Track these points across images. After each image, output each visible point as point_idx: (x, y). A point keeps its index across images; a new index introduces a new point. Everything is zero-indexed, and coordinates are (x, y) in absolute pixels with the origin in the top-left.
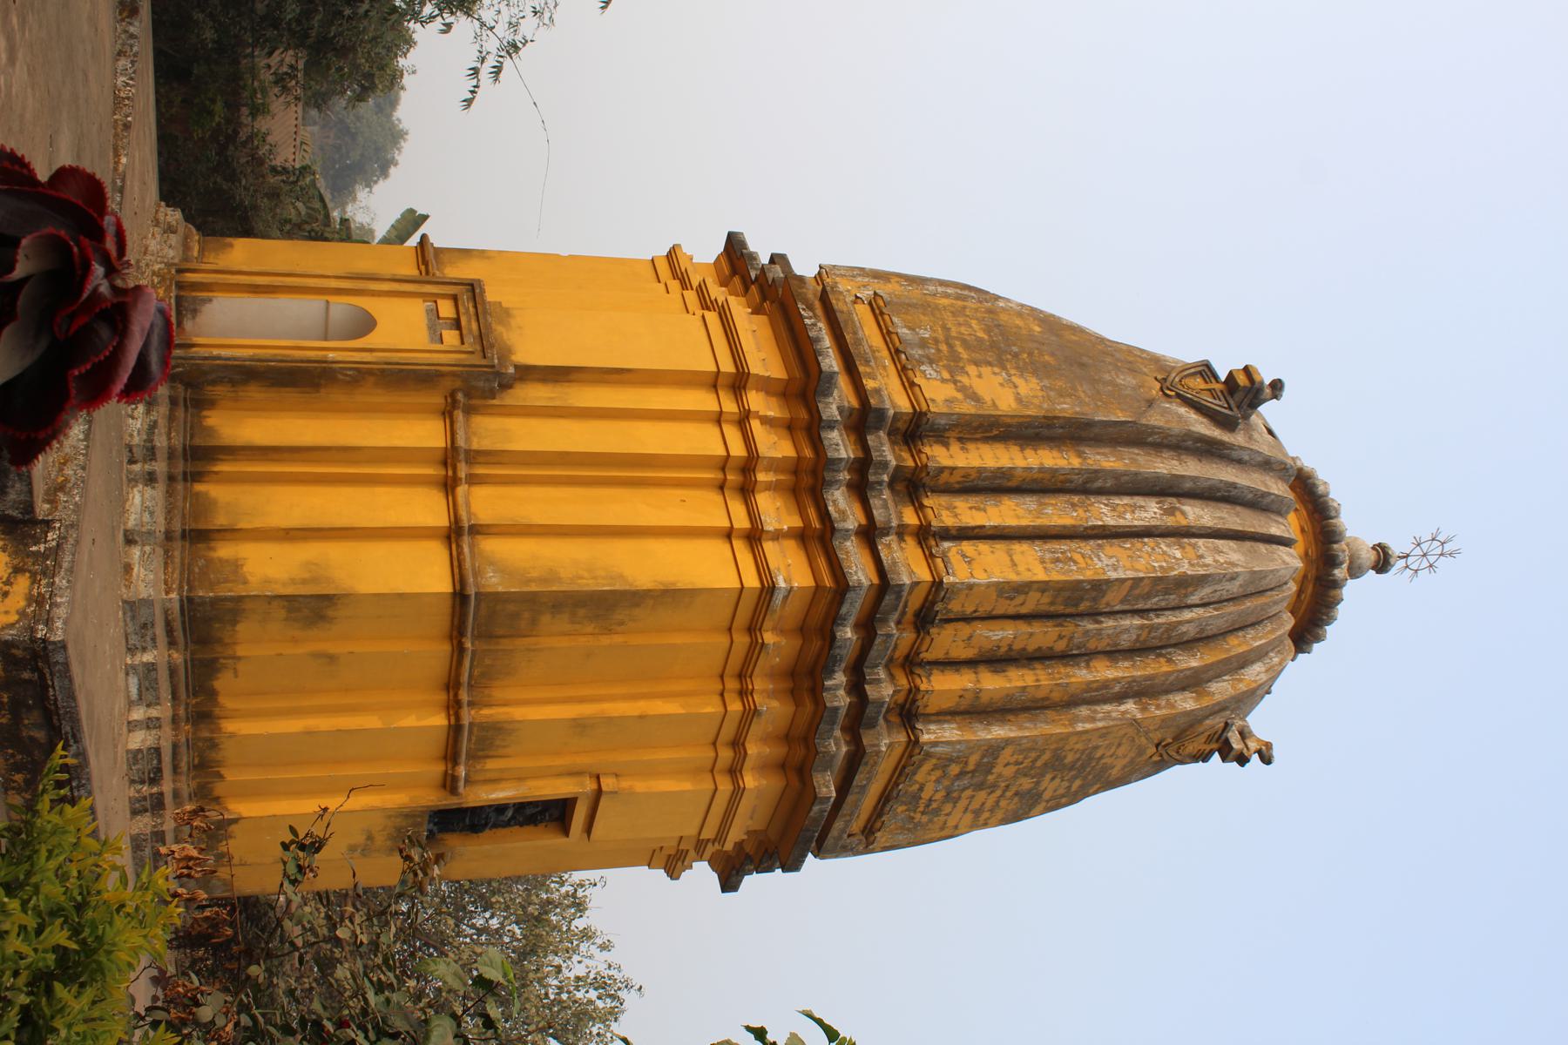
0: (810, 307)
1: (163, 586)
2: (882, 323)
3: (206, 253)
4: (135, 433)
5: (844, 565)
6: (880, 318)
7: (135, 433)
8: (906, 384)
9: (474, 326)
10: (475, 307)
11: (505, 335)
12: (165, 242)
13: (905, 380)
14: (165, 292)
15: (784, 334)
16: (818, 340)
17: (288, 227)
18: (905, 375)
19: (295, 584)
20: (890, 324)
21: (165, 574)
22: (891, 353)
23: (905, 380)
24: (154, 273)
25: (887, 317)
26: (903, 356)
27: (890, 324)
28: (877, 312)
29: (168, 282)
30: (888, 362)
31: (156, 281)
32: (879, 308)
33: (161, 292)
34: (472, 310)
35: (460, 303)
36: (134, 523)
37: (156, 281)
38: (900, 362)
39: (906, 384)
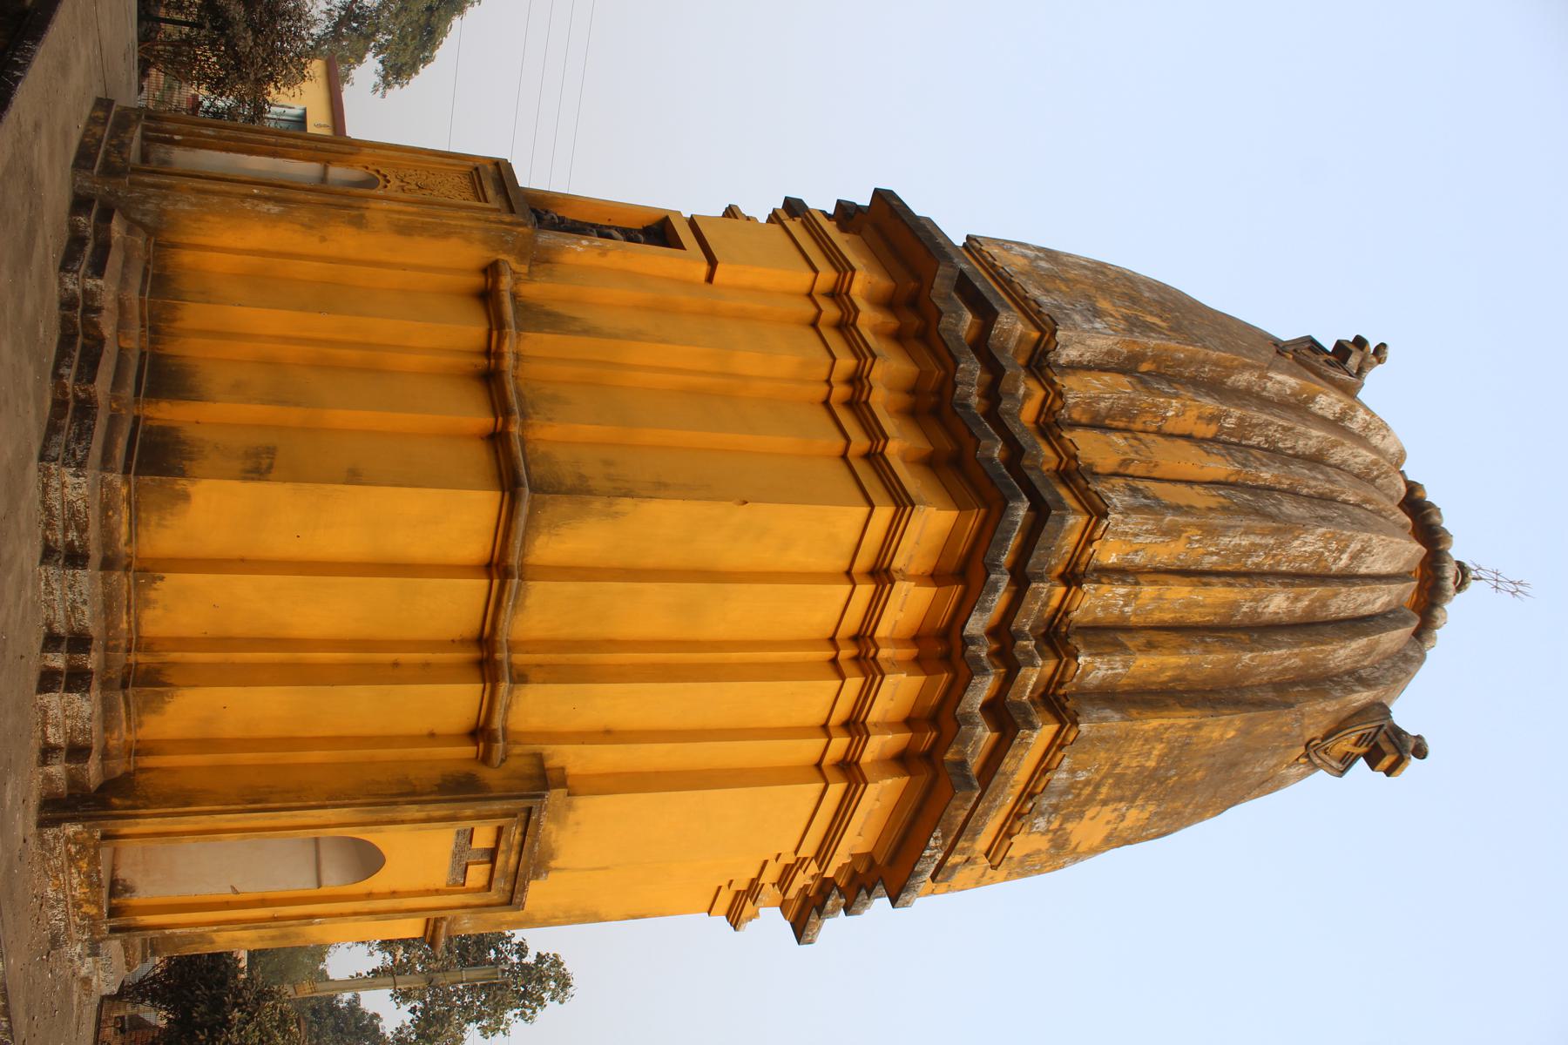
0: (945, 836)
1: (125, 967)
2: (1049, 757)
3: (143, 515)
4: (76, 958)
5: (809, 927)
6: (1054, 749)
7: (76, 958)
8: (1005, 829)
9: (513, 860)
10: (524, 834)
11: (553, 836)
12: (71, 587)
13: (1008, 824)
14: (88, 865)
15: (906, 814)
16: (921, 873)
17: (265, 1038)
18: (1013, 822)
19: (262, 940)
20: (1055, 765)
21: (126, 957)
22: (1024, 790)
23: (1008, 824)
24: (68, 840)
25: (1059, 755)
26: (1030, 805)
27: (1055, 765)
28: (1058, 742)
29: (92, 851)
30: (1011, 800)
31: (73, 850)
32: (1064, 738)
33: (84, 865)
34: (518, 837)
35: (504, 837)
36: (87, 971)
37: (73, 850)
38: (1022, 807)
39: (1005, 829)
